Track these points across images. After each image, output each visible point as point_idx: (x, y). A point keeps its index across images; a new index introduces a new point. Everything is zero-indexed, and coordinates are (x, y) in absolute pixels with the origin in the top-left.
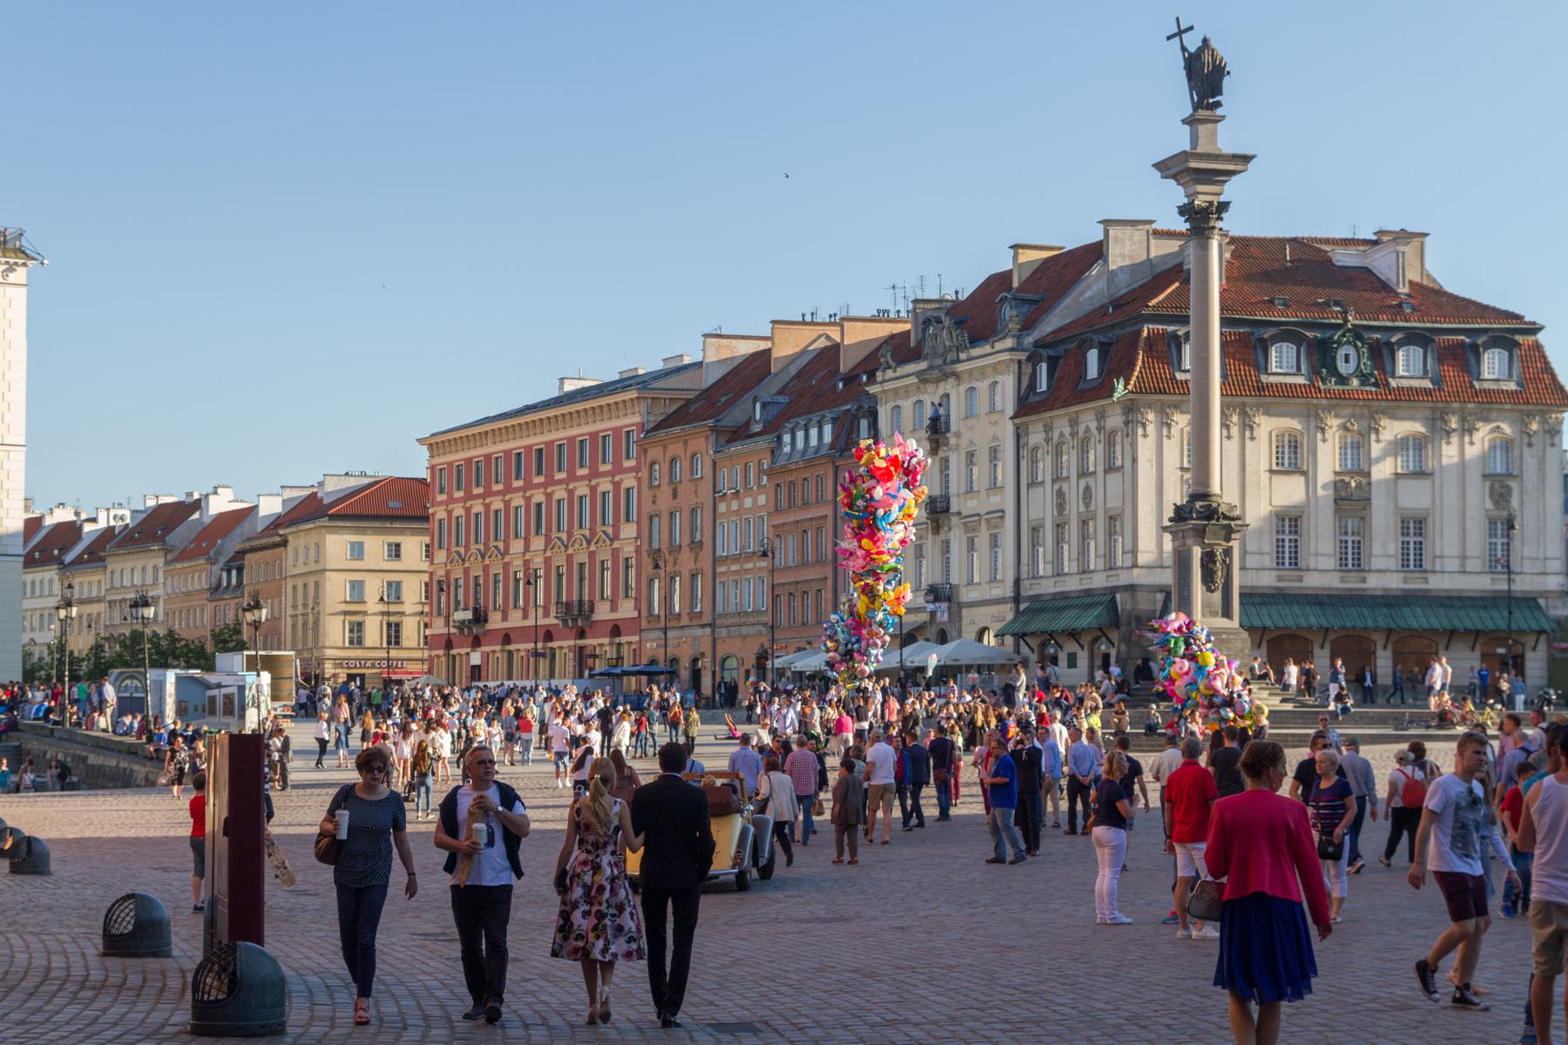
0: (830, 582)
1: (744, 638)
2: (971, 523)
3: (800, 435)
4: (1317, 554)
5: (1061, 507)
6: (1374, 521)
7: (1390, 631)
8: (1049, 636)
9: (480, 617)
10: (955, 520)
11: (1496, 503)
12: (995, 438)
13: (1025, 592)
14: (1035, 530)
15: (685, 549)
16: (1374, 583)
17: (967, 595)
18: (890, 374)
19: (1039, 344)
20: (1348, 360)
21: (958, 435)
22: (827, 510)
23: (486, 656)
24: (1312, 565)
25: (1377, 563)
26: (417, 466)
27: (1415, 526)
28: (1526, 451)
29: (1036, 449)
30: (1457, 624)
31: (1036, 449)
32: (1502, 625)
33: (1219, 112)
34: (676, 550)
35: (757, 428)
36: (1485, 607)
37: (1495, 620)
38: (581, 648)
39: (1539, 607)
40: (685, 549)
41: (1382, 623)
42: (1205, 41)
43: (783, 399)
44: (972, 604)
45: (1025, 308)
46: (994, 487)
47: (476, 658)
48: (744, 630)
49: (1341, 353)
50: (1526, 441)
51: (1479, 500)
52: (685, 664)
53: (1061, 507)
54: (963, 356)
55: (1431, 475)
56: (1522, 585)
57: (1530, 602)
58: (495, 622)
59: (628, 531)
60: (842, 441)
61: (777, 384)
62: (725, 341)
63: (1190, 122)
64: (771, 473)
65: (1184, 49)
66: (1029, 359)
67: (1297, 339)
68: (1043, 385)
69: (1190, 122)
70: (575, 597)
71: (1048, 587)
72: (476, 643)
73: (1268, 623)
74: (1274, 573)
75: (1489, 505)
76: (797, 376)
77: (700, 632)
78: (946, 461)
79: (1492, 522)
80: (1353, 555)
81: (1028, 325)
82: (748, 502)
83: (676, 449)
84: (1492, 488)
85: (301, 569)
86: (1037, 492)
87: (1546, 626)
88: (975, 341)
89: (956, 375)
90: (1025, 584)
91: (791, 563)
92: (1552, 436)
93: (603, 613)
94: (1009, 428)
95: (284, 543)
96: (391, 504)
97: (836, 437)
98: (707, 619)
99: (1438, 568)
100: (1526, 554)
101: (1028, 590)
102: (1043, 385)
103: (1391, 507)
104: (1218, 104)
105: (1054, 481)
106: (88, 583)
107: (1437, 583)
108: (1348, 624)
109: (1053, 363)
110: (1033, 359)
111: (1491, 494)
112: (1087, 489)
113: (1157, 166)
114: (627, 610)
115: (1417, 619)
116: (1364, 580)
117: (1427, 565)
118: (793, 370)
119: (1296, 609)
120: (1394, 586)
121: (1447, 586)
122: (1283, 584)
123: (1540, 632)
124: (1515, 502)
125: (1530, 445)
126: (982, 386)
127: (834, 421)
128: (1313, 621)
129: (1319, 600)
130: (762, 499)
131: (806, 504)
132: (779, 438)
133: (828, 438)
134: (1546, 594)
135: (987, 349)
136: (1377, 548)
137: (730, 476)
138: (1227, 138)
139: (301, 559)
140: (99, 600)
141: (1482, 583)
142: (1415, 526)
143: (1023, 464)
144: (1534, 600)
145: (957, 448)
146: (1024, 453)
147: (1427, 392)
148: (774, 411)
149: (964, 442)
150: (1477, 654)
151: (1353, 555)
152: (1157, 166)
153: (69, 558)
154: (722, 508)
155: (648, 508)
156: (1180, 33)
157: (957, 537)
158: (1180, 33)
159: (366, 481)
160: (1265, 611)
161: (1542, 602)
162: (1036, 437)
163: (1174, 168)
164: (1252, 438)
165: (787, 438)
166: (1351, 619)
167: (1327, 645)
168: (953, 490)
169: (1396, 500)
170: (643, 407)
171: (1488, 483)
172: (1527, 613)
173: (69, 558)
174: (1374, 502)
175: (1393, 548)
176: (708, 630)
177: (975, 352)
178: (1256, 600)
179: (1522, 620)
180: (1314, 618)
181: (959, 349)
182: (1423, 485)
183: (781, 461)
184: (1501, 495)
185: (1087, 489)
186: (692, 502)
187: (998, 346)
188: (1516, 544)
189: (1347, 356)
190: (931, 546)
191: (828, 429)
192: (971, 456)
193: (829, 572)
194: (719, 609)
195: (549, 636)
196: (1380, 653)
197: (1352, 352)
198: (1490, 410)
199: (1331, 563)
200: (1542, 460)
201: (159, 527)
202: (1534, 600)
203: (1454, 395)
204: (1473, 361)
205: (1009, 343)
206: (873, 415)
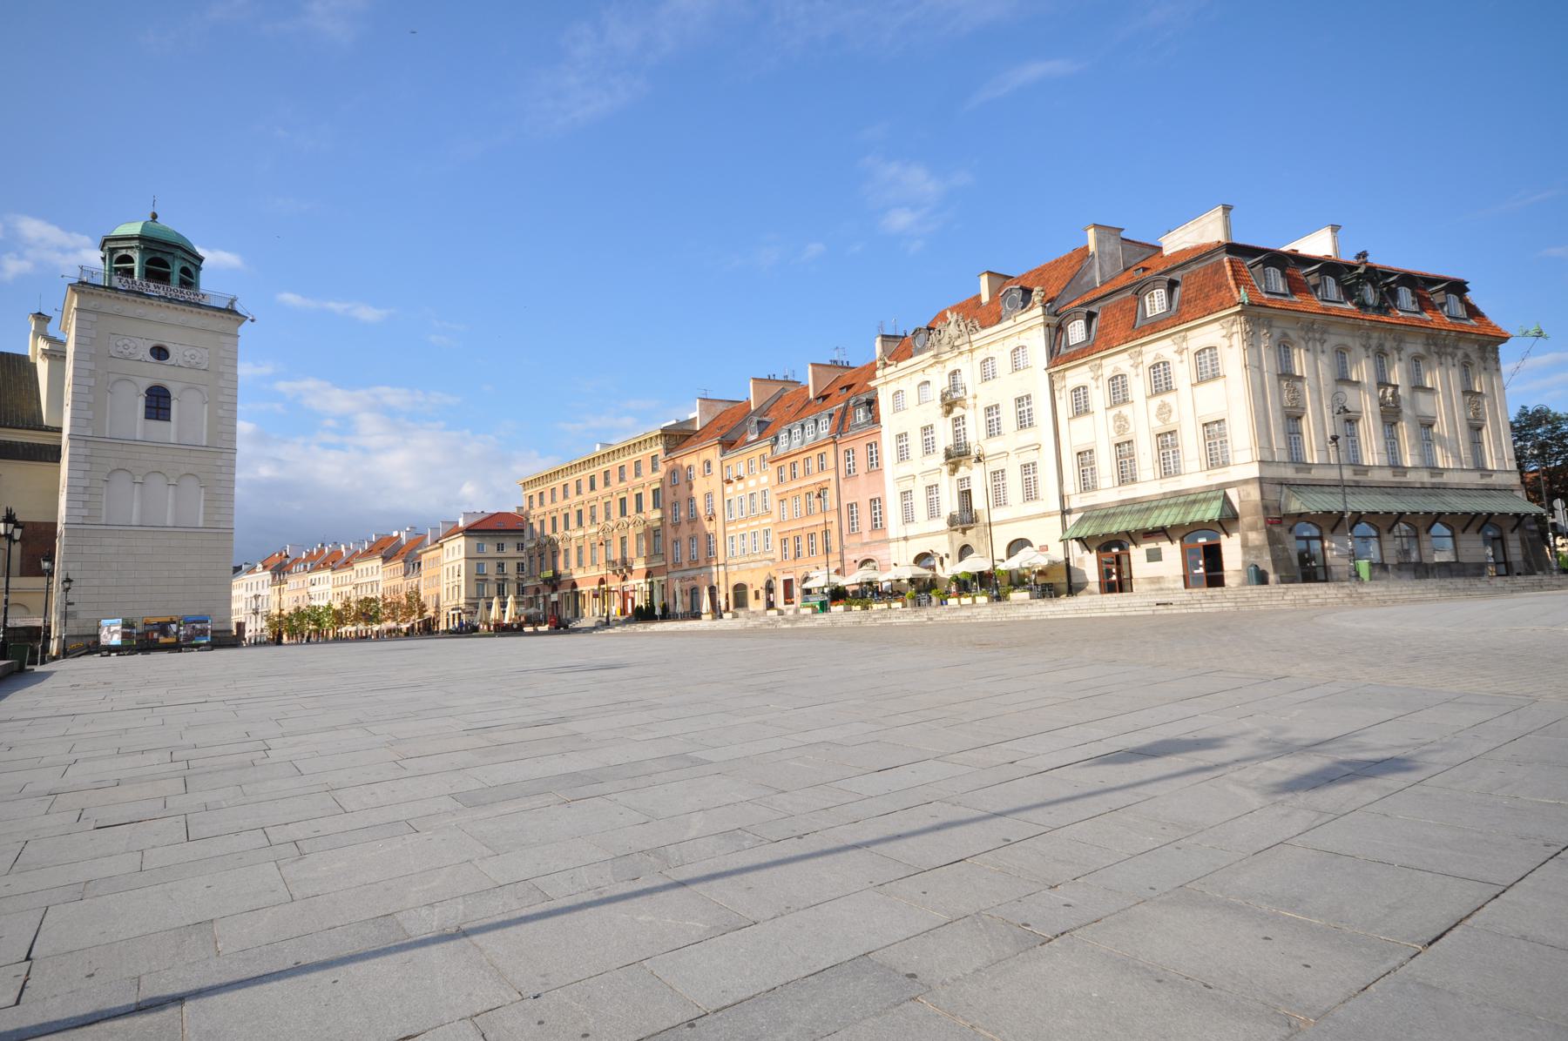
1: (753, 570)
22: (832, 476)
48: (752, 565)
85: (451, 558)
106: (345, 575)
127: (831, 416)
132: (777, 439)
165: (783, 436)
206: (871, 404)
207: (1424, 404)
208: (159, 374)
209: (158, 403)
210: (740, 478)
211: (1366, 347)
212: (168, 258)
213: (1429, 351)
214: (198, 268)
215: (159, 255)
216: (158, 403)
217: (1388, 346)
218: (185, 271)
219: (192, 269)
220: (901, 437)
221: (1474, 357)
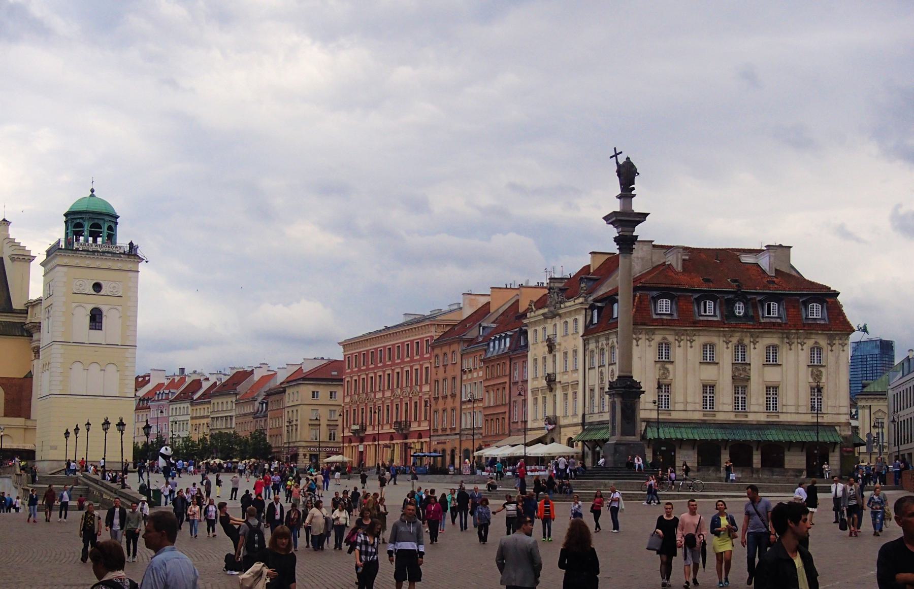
0: (507, 414)
2: (565, 387)
3: (497, 342)
5: (602, 379)
6: (752, 388)
7: (759, 442)
8: (597, 443)
9: (363, 428)
10: (558, 386)
12: (575, 346)
13: (587, 421)
14: (592, 390)
15: (449, 397)
16: (752, 418)
17: (563, 422)
18: (533, 314)
19: (596, 300)
20: (740, 309)
21: (560, 344)
22: (507, 380)
23: (365, 447)
24: (721, 409)
26: (338, 354)
27: (772, 390)
28: (830, 353)
29: (592, 351)
30: (793, 438)
31: (592, 351)
32: (816, 440)
33: (633, 193)
34: (445, 397)
35: (481, 339)
36: (807, 430)
37: (810, 437)
38: (406, 444)
39: (836, 430)
40: (449, 397)
41: (755, 437)
42: (628, 158)
43: (494, 325)
44: (565, 426)
45: (591, 283)
46: (576, 370)
47: (361, 449)
51: (805, 379)
52: (448, 452)
53: (602, 379)
54: (562, 306)
56: (826, 419)
57: (831, 427)
58: (370, 431)
59: (426, 388)
60: (513, 347)
61: (493, 318)
62: (473, 297)
63: (619, 197)
64: (484, 361)
65: (617, 163)
66: (590, 308)
67: (714, 300)
68: (595, 321)
69: (619, 197)
70: (404, 419)
71: (596, 418)
72: (362, 440)
73: (697, 437)
75: (811, 380)
76: (502, 314)
77: (454, 437)
78: (555, 356)
79: (812, 388)
80: (740, 403)
81: (590, 292)
82: (475, 375)
83: (446, 349)
84: (812, 372)
86: (592, 371)
87: (838, 440)
88: (569, 298)
89: (560, 315)
90: (587, 417)
91: (492, 404)
92: (843, 346)
93: (414, 427)
94: (581, 340)
95: (284, 391)
96: (334, 373)
97: (511, 343)
98: (457, 431)
99: (784, 411)
100: (830, 404)
101: (588, 420)
102: (595, 321)
103: (761, 380)
104: (633, 189)
105: (610, 365)
107: (783, 418)
108: (737, 438)
109: (600, 309)
110: (592, 307)
112: (612, 371)
113: (606, 218)
114: (425, 426)
115: (773, 436)
116: (747, 416)
117: (779, 409)
118: (501, 311)
119: (712, 431)
121: (789, 420)
123: (836, 443)
124: (823, 380)
125: (832, 351)
126: (570, 320)
128: (720, 437)
129: (723, 426)
130: (481, 373)
131: (498, 377)
132: (489, 344)
133: (508, 345)
134: (839, 424)
135: (572, 303)
136: (753, 401)
137: (468, 363)
138: (637, 206)
139: (291, 399)
140: (208, 417)
141: (809, 418)
142: (772, 390)
143: (587, 358)
144: (833, 426)
145: (560, 350)
146: (587, 353)
147: (780, 324)
148: (489, 331)
149: (562, 348)
150: (804, 453)
151: (740, 403)
152: (606, 218)
153: (195, 397)
154: (465, 377)
155: (434, 377)
156: (616, 155)
157: (559, 393)
158: (616, 155)
159: (323, 362)
160: (695, 431)
161: (837, 428)
162: (592, 346)
163: (612, 219)
165: (492, 344)
166: (740, 436)
167: (728, 448)
168: (558, 371)
170: (433, 329)
172: (829, 433)
173: (195, 397)
174: (752, 378)
175: (762, 400)
176: (458, 436)
177: (568, 304)
178: (692, 425)
179: (825, 437)
180: (720, 436)
181: (561, 303)
182: (778, 369)
183: (489, 355)
184: (817, 375)
185: (612, 371)
186: (453, 374)
187: (577, 301)
188: (824, 399)
190: (549, 397)
191: (508, 340)
192: (566, 353)
193: (507, 409)
194: (463, 427)
195: (392, 439)
196: (755, 452)
197: (741, 305)
198: (811, 333)
199: (730, 408)
200: (838, 358)
201: (235, 382)
203: (794, 327)
204: (803, 310)
205: (581, 300)
207: (772, 375)
208: (96, 301)
209: (96, 318)
210: (470, 371)
211: (727, 343)
212: (101, 222)
213: (782, 342)
214: (116, 223)
215: (96, 221)
216: (96, 318)
217: (746, 341)
218: (110, 228)
219: (113, 225)
220: (535, 360)
221: (823, 342)
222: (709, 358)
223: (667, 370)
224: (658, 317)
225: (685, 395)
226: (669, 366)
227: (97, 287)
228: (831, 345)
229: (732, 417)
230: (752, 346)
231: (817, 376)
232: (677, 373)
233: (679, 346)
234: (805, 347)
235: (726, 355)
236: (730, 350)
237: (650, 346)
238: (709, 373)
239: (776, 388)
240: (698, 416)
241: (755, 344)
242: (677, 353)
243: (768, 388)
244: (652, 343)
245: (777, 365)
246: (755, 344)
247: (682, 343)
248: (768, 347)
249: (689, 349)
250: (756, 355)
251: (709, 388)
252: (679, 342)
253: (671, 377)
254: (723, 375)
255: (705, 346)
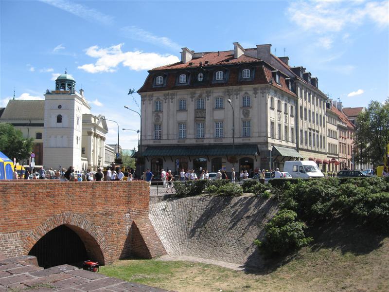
4: (189, 134)
11: (245, 116)
20: (200, 78)
24: (188, 137)
25: (207, 136)
49: (199, 75)
50: (254, 96)
51: (239, 114)
55: (224, 108)
56: (253, 140)
74: (177, 140)
75: (243, 117)
84: (243, 111)
103: (212, 118)
111: (243, 113)
120: (212, 143)
122: (179, 143)
125: (255, 97)
134: (259, 143)
144: (256, 145)
161: (259, 146)
164: (172, 102)
169: (213, 116)
171: (242, 110)
184: (246, 113)
189: (201, 76)
197: (202, 75)
199: (192, 136)
202: (256, 145)
207: (219, 115)
209: (59, 119)
211: (192, 98)
216: (59, 119)
217: (204, 95)
221: (251, 93)
222: (182, 109)
223: (159, 116)
224: (156, 87)
225: (168, 131)
226: (160, 114)
227: (60, 107)
228: (255, 93)
229: (194, 142)
230: (207, 99)
231: (246, 114)
232: (164, 116)
233: (166, 102)
234: (238, 96)
235: (191, 106)
236: (194, 102)
237: (150, 103)
238: (182, 116)
239: (222, 122)
240: (175, 142)
241: (208, 97)
242: (165, 106)
243: (217, 124)
244: (151, 102)
245: (221, 108)
246: (208, 97)
247: (167, 101)
248: (217, 99)
249: (171, 103)
250: (209, 104)
251: (181, 124)
252: (166, 100)
253: (161, 120)
254: (189, 116)
255: (180, 101)
